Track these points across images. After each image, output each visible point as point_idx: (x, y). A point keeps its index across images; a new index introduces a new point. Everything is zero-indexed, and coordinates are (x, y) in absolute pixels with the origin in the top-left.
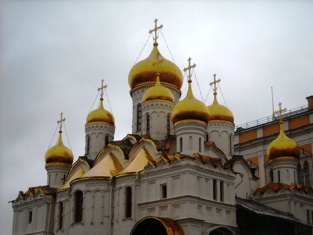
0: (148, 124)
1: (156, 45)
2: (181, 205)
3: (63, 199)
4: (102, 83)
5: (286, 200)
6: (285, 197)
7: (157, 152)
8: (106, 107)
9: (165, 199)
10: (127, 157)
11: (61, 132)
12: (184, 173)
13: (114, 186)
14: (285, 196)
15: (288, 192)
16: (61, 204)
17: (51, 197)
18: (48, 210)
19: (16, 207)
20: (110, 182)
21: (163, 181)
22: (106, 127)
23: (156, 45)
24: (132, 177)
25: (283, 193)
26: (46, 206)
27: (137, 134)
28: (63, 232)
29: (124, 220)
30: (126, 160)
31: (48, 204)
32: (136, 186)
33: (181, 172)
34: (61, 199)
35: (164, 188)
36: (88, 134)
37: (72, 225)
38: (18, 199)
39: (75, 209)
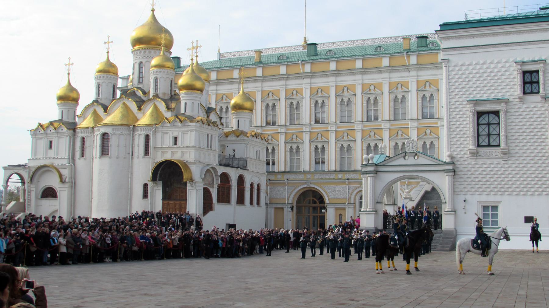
0: (156, 86)
1: (153, 10)
2: (189, 152)
3: (84, 135)
4: (109, 38)
5: (244, 143)
6: (244, 141)
7: (167, 110)
8: (112, 60)
9: (176, 146)
10: (139, 108)
11: (69, 74)
12: (191, 131)
13: (133, 132)
14: (244, 140)
15: (246, 138)
16: (83, 139)
17: (72, 131)
18: (70, 142)
19: (34, 135)
20: (131, 129)
21: (175, 134)
22: (114, 78)
23: (153, 10)
24: (150, 128)
25: (242, 138)
26: (68, 138)
27: (139, 86)
28: (85, 160)
29: (143, 157)
30: (139, 111)
31: (70, 137)
32: (153, 134)
33: (190, 130)
34: (82, 134)
35: (176, 139)
36: (98, 81)
37: (100, 157)
38: (37, 129)
39: (101, 146)
